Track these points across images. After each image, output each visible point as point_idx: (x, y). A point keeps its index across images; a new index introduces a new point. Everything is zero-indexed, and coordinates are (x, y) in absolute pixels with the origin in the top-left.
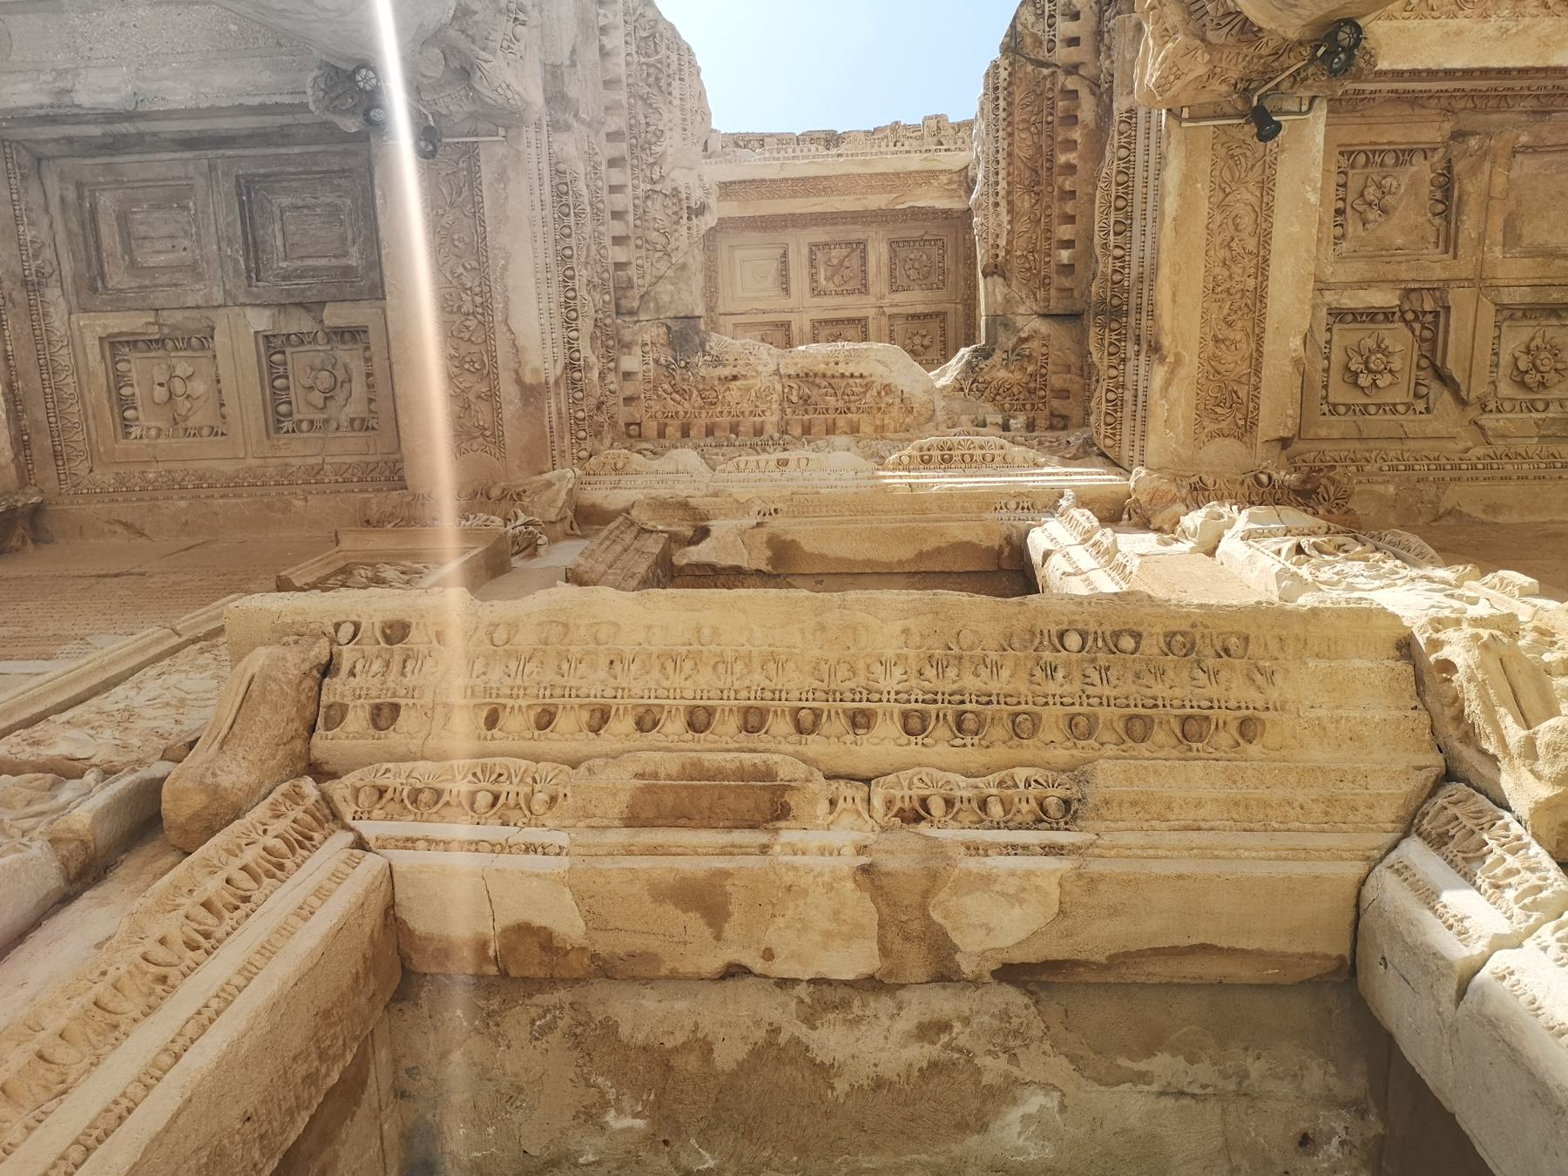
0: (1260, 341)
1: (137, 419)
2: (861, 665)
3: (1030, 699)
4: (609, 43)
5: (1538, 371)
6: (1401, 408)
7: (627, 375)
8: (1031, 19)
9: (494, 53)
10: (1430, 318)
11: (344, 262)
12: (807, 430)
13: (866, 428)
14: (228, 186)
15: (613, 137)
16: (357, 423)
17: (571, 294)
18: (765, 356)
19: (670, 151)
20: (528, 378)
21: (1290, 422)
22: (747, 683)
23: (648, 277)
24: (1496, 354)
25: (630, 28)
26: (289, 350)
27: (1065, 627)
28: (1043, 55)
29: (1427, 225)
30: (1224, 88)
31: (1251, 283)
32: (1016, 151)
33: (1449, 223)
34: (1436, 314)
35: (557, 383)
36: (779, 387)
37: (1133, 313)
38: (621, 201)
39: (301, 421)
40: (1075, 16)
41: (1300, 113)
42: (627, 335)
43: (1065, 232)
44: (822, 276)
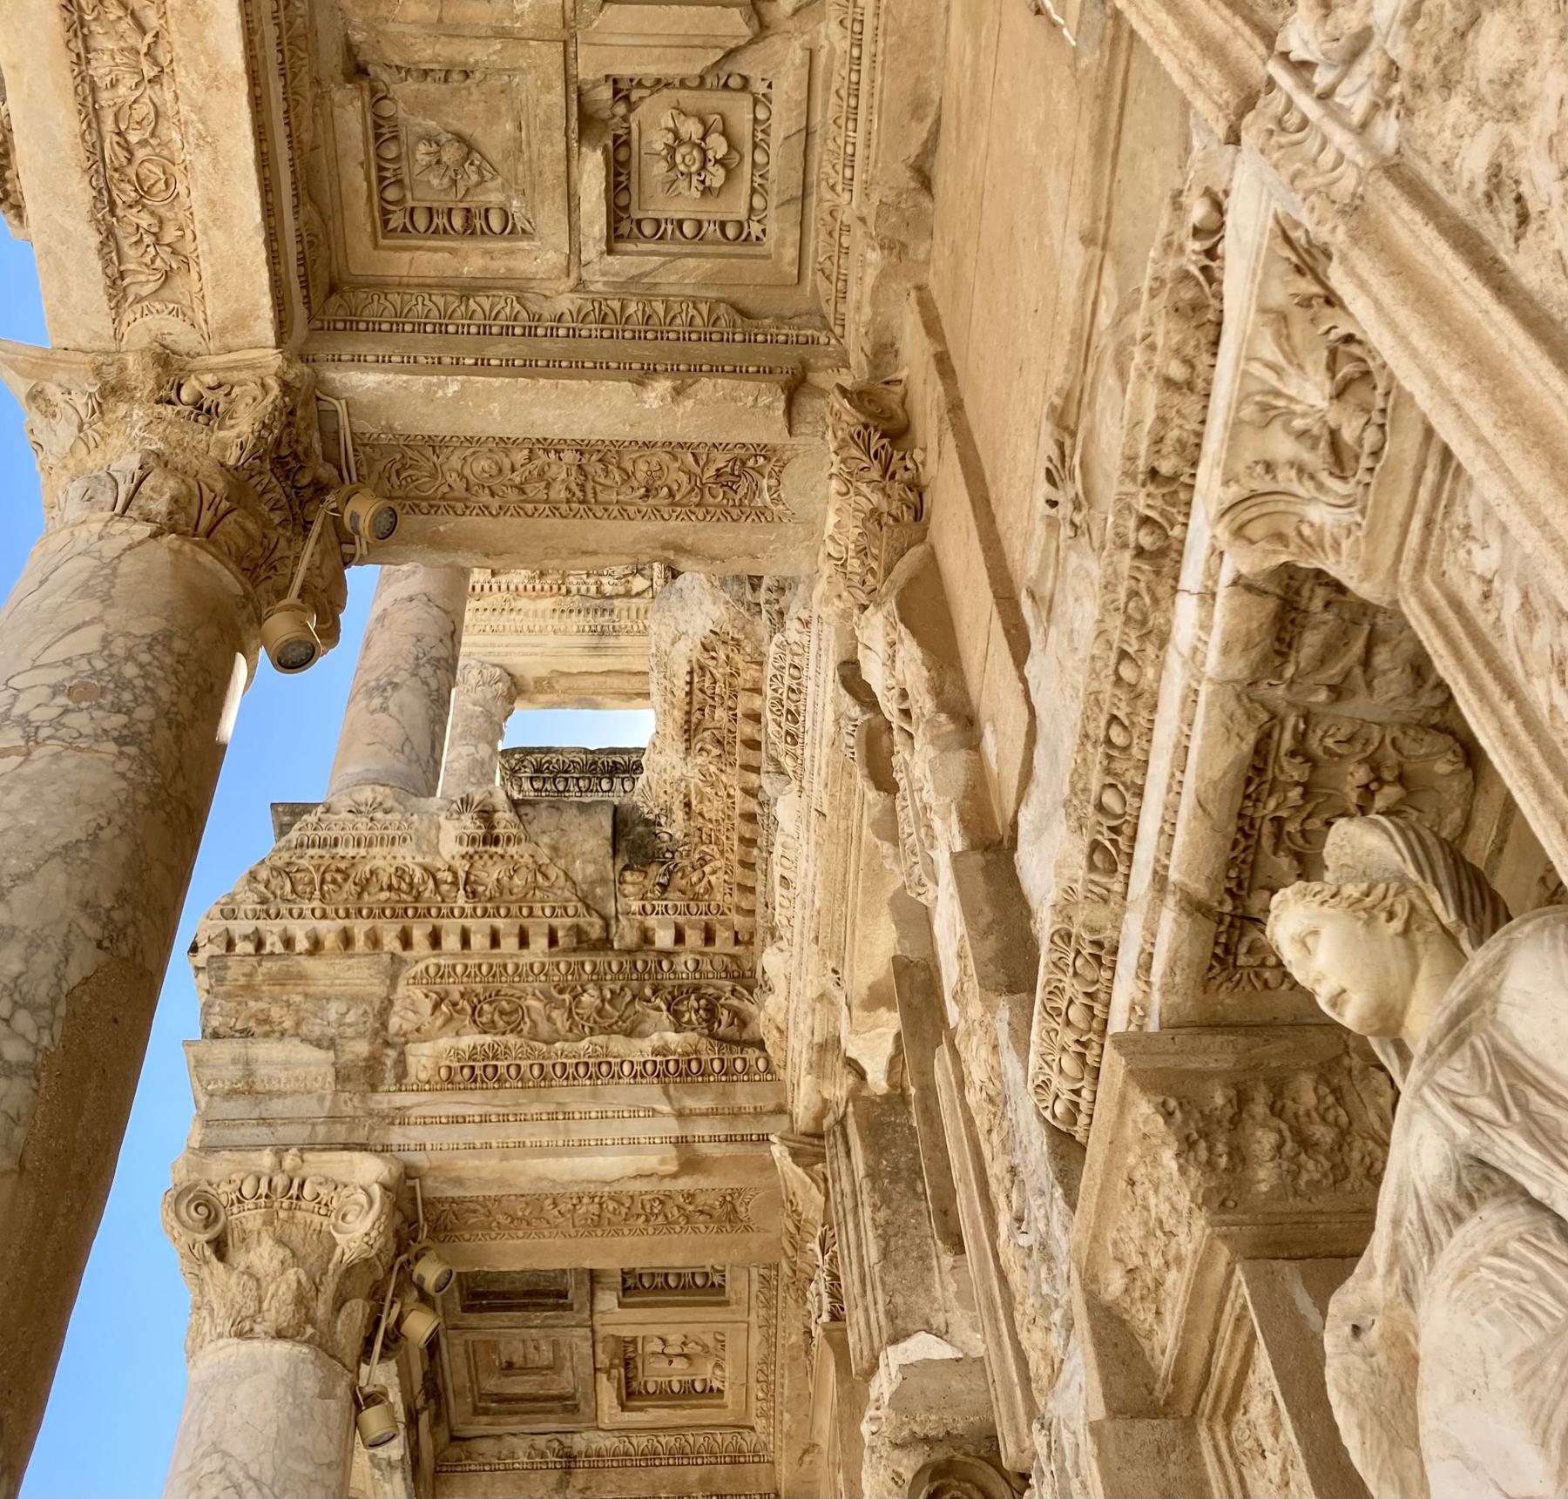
4: (302, 944)
7: (680, 938)
14: (473, 1319)
15: (406, 941)
17: (582, 1070)
19: (419, 859)
20: (673, 1167)
29: (484, 87)
36: (699, 760)
38: (479, 941)
42: (631, 938)
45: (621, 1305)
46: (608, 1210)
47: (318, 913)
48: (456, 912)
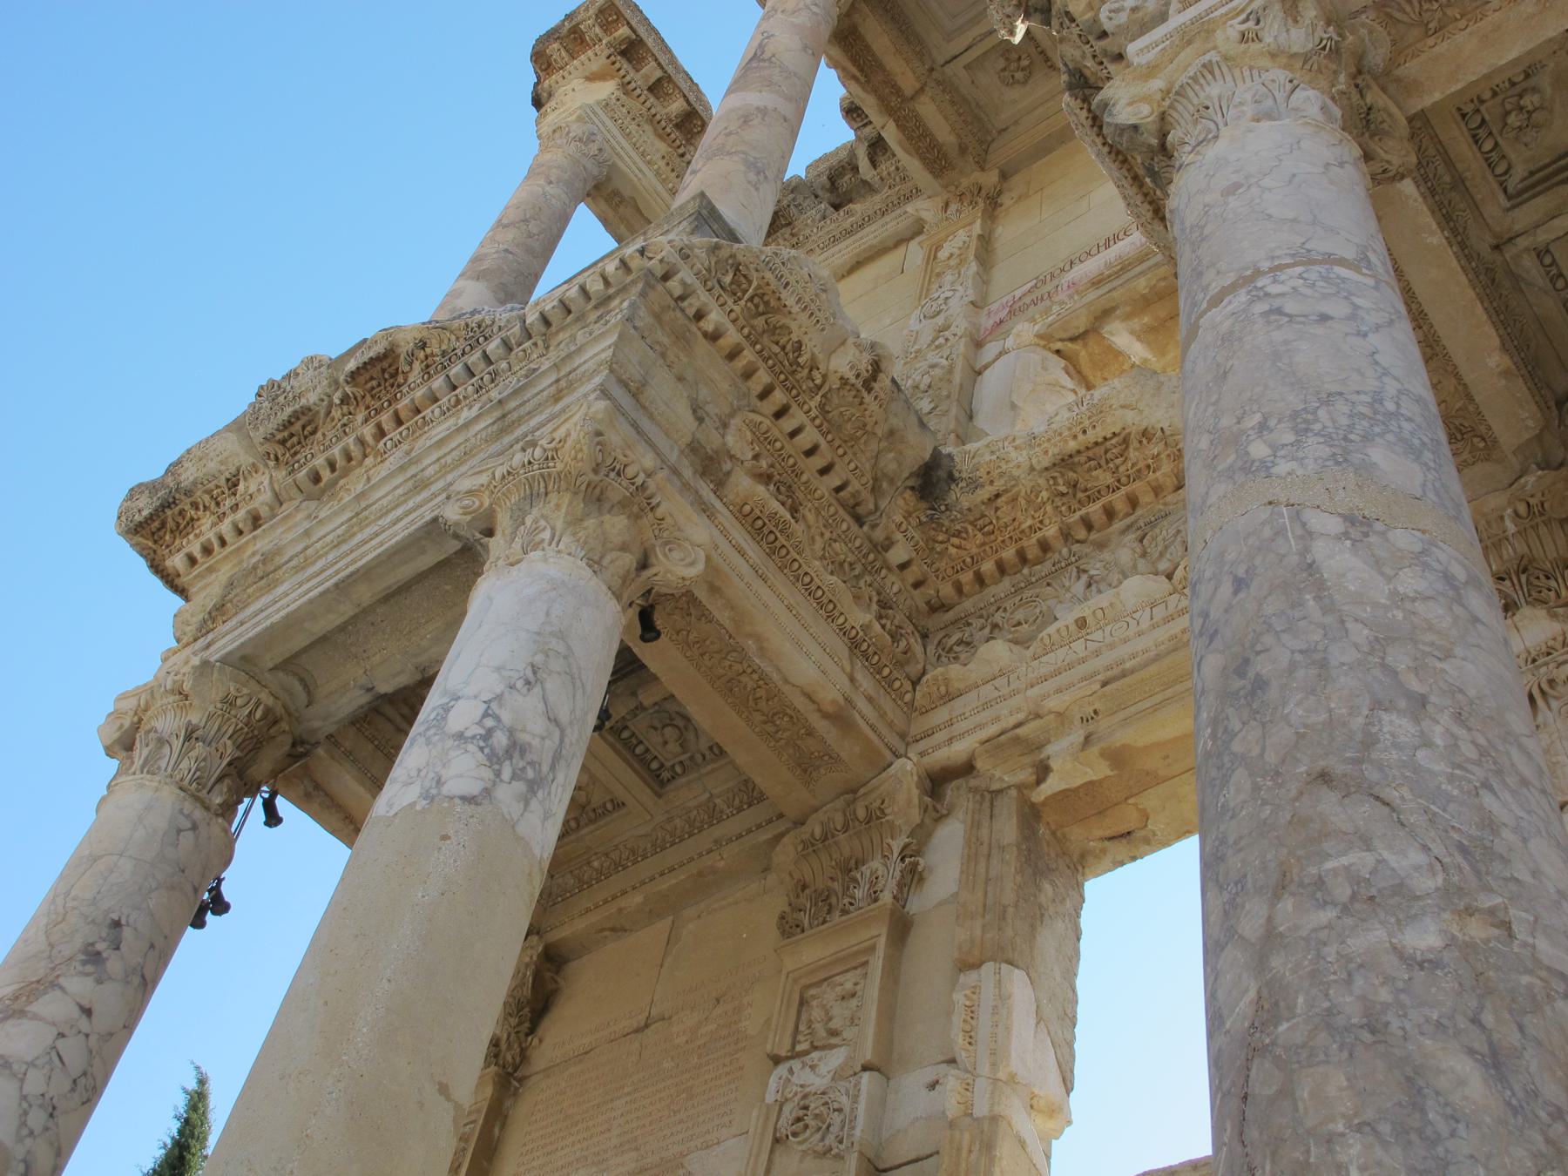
0: (1457, 376)
4: (708, 325)
7: (903, 567)
15: (765, 394)
18: (1014, 454)
21: (1530, 423)
36: (1041, 481)
42: (879, 535)
47: (733, 315)
48: (806, 407)
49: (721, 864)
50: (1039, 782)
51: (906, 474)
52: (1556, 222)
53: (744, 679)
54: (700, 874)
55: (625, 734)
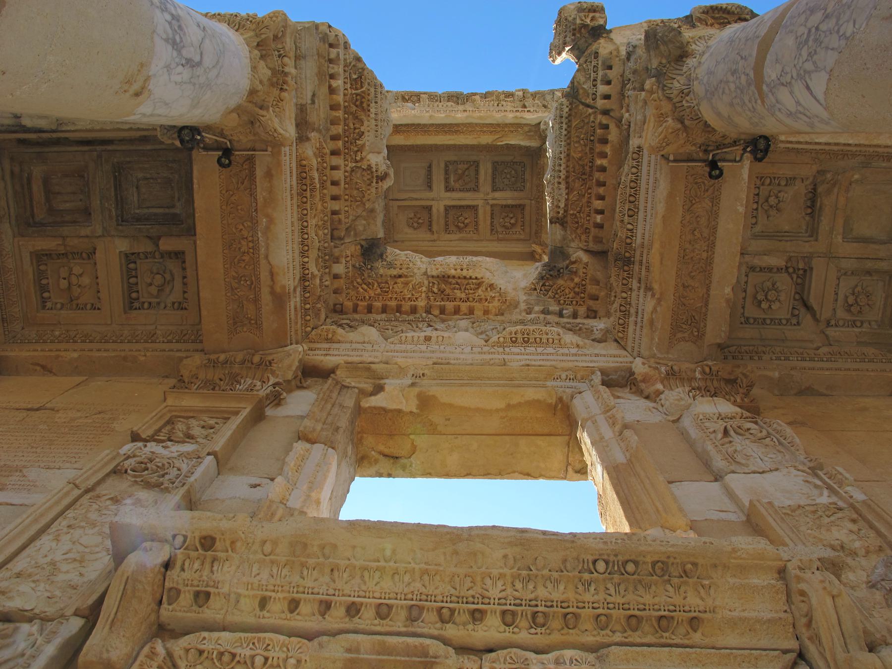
1: (50, 298)
2: (479, 579)
3: (575, 604)
4: (334, 83)
5: (858, 305)
6: (784, 322)
7: (336, 277)
8: (583, 80)
9: (267, 109)
10: (801, 272)
11: (172, 211)
12: (443, 311)
13: (478, 313)
15: (334, 138)
16: (176, 305)
17: (306, 236)
18: (419, 263)
21: (723, 334)
22: (412, 589)
23: (351, 217)
24: (837, 294)
25: (347, 74)
26: (138, 262)
27: (597, 557)
28: (589, 101)
30: (693, 148)
31: (705, 255)
32: (572, 154)
33: (814, 220)
34: (805, 271)
35: (295, 290)
36: (426, 282)
37: (637, 264)
39: (144, 303)
40: (609, 83)
41: (735, 161)
42: (336, 252)
43: (598, 204)
44: (452, 179)
45: (120, 252)
46: (244, 254)
49: (143, 358)
50: (373, 394)
51: (363, 237)
52: (766, 257)
53: (244, 243)
54: (125, 358)
55: (132, 266)
